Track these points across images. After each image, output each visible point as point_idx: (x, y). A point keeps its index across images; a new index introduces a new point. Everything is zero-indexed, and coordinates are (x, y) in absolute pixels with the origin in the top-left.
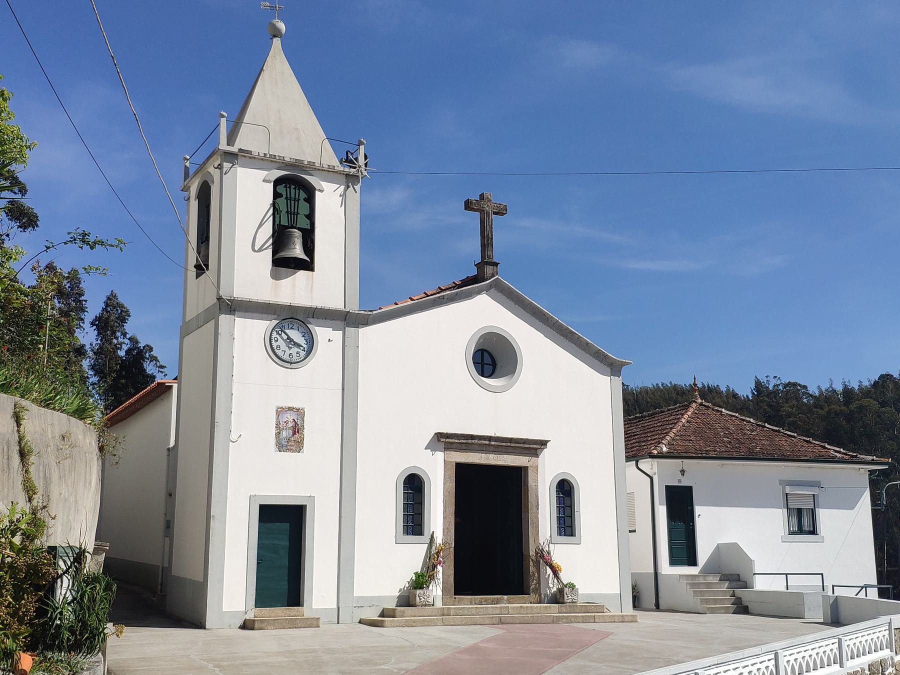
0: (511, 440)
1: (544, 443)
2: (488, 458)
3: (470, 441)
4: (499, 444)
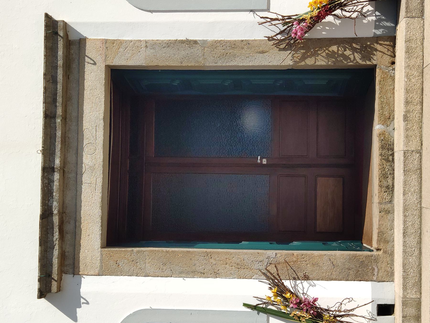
0: (49, 117)
1: (54, 29)
2: (92, 168)
3: (56, 220)
4: (58, 146)
